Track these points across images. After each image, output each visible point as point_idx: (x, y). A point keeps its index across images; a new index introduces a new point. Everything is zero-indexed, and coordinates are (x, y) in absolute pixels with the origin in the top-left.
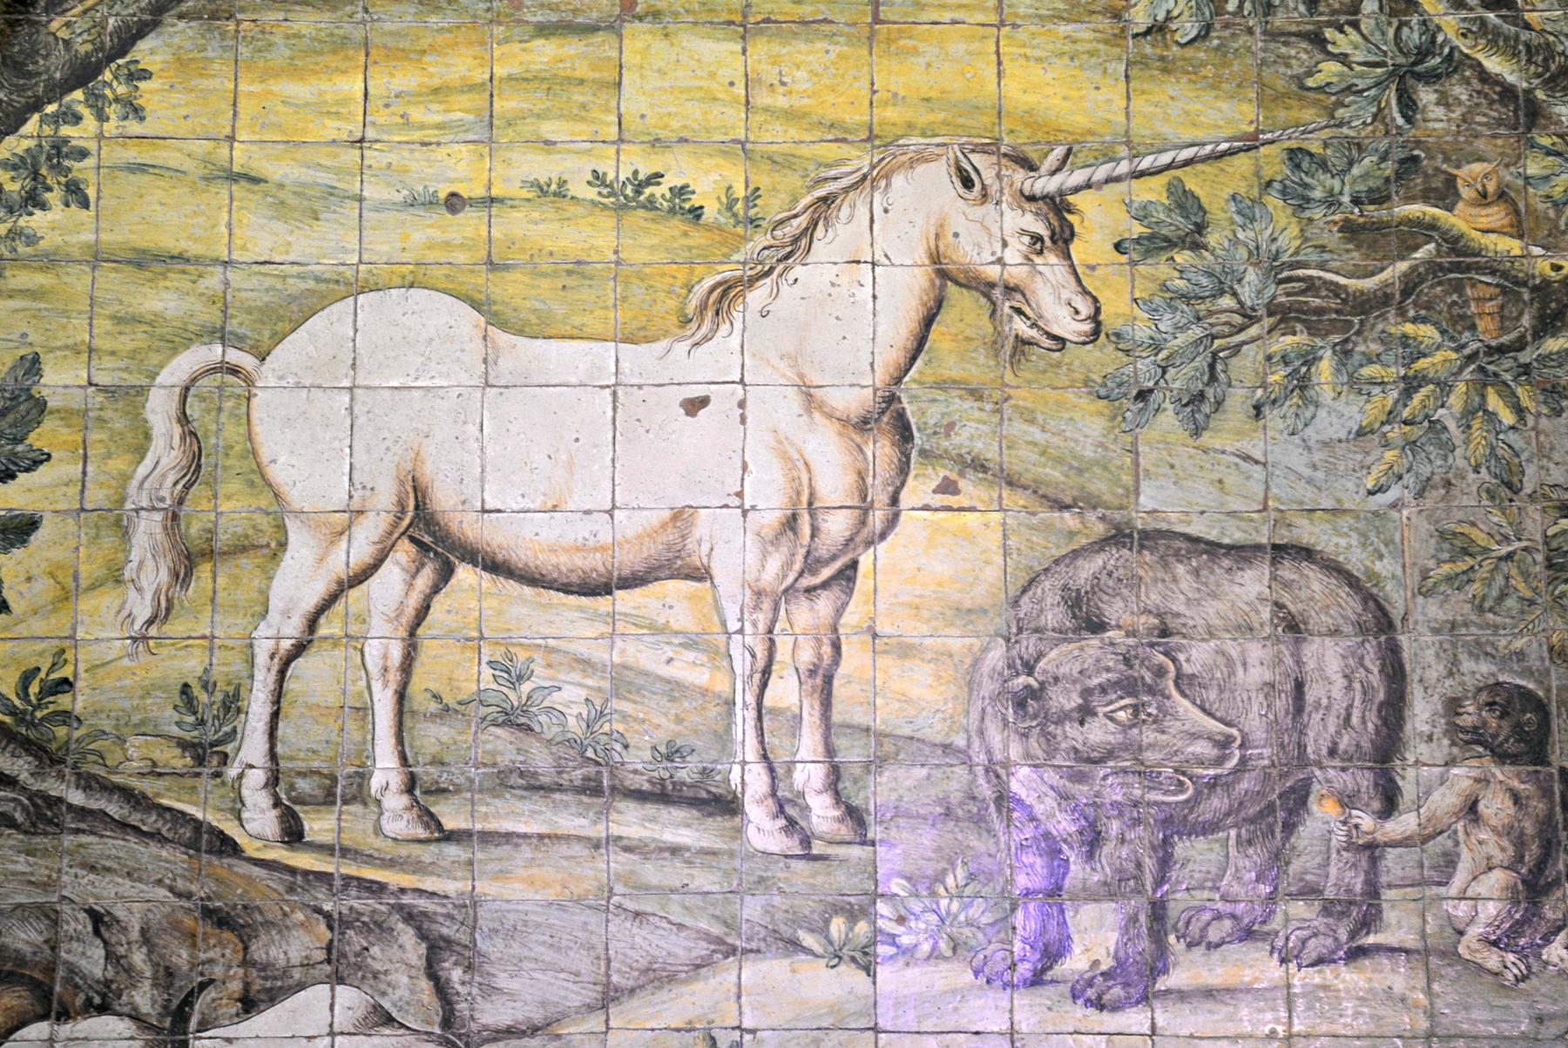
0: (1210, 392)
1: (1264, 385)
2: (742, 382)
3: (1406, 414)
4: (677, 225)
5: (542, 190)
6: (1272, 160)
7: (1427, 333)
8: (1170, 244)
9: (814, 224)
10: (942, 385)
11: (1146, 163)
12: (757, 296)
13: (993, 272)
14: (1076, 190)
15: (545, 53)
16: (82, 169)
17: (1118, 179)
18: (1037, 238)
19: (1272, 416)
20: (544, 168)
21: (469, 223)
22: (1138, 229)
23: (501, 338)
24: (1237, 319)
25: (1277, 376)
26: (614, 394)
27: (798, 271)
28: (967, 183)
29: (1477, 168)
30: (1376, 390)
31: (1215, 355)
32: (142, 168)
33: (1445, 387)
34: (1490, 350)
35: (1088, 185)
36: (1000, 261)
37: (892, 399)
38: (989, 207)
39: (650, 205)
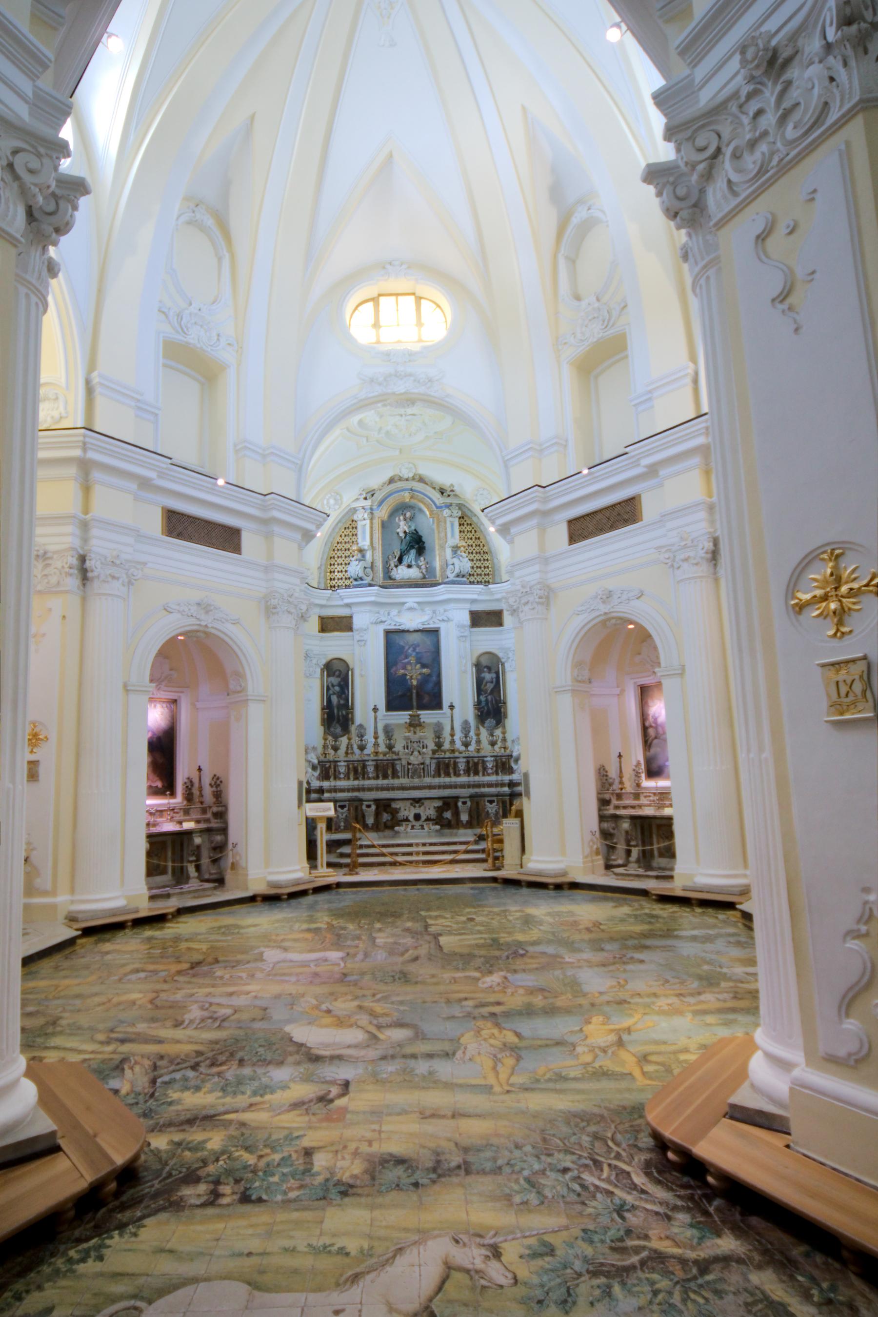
0: (570, 1299)
1: (592, 1295)
2: (361, 1303)
3: (657, 1301)
4: (339, 1257)
5: (286, 1250)
6: (577, 1232)
7: (655, 1276)
8: (541, 1255)
9: (394, 1257)
10: (450, 1301)
11: (527, 1234)
12: (369, 1277)
13: (470, 1267)
14: (501, 1242)
15: (295, 1215)
16: (105, 1251)
17: (517, 1239)
18: (487, 1257)
19: (597, 1305)
20: (287, 1243)
21: (253, 1260)
22: (527, 1252)
23: (256, 1293)
24: (575, 1276)
25: (597, 1292)
26: (303, 1310)
27: (388, 1268)
28: (457, 1242)
29: (655, 1231)
30: (641, 1295)
31: (568, 1288)
32: (130, 1250)
33: (670, 1293)
34: (684, 1280)
35: (506, 1241)
36: (473, 1263)
37: (427, 1308)
38: (467, 1249)
39: (329, 1252)
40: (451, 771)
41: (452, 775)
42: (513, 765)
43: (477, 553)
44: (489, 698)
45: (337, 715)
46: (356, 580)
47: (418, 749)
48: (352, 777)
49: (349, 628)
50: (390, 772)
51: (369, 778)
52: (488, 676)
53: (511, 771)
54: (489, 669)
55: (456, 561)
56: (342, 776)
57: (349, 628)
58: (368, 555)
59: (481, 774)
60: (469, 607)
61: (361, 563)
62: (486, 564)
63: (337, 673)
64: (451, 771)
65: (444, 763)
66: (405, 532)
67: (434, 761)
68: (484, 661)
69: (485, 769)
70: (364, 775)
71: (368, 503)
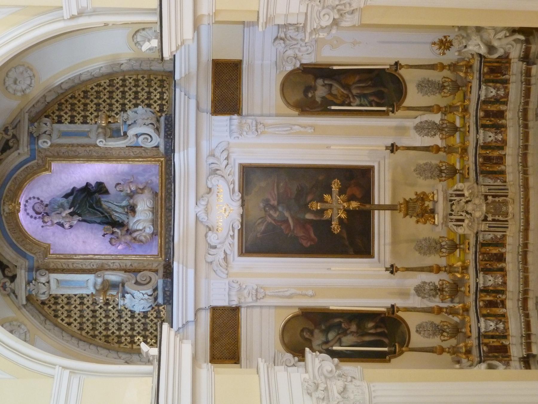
40: (496, 153)
41: (502, 152)
42: (495, 56)
43: (111, 98)
44: (355, 92)
45: (374, 336)
46: (156, 299)
47: (462, 203)
48: (501, 311)
49: (234, 312)
50: (495, 251)
51: (504, 283)
52: (321, 92)
53: (505, 59)
54: (309, 88)
55: (131, 132)
56: (501, 326)
57: (234, 312)
58: (114, 277)
59: (503, 108)
60: (206, 117)
61: (127, 288)
62: (130, 82)
63: (306, 335)
64: (496, 153)
65: (482, 164)
66: (72, 214)
67: (481, 179)
68: (298, 96)
69: (497, 101)
70: (499, 291)
71: (22, 276)
